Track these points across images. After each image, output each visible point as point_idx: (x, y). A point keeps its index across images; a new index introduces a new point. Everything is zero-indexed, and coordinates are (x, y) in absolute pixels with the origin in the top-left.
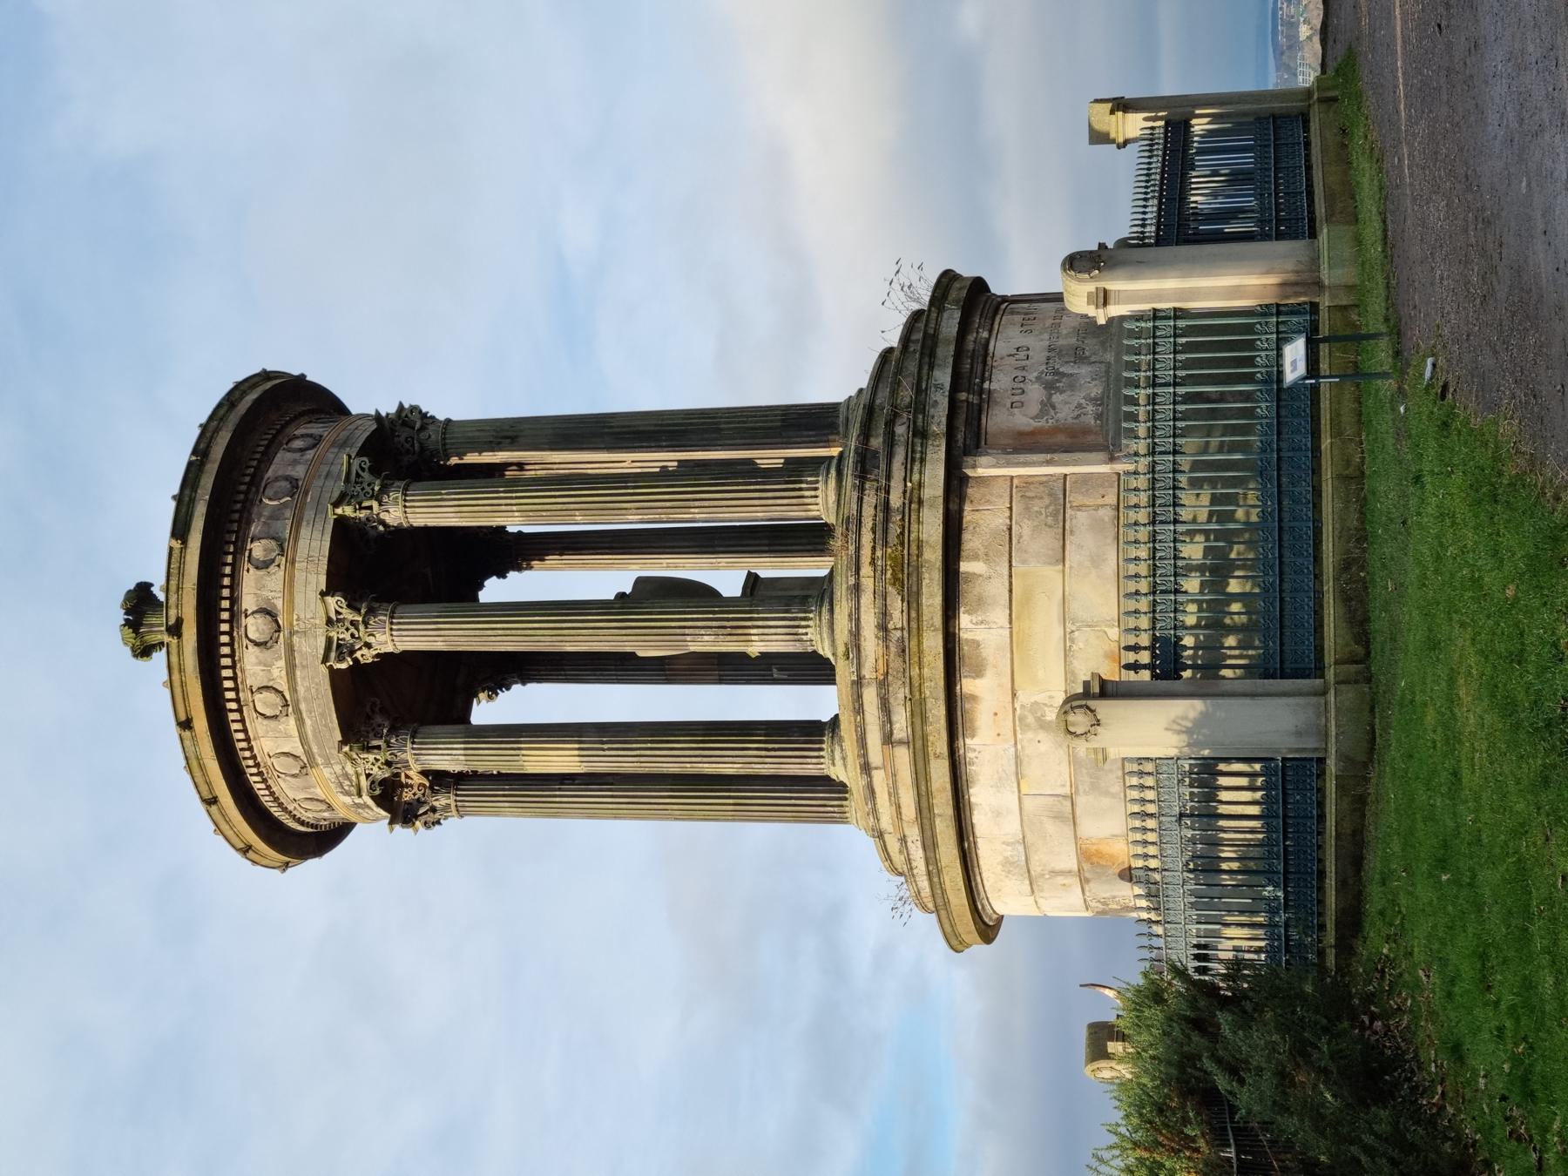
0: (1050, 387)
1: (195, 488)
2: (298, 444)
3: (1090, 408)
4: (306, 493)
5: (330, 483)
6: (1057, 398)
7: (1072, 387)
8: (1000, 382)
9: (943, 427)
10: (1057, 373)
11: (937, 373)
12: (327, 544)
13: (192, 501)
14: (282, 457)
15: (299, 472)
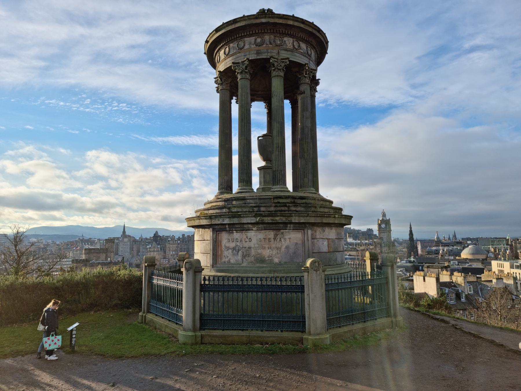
0: (234, 249)
1: (227, 26)
2: (259, 40)
3: (227, 260)
4: (239, 53)
5: (243, 57)
6: (230, 251)
7: (234, 255)
8: (236, 235)
9: (213, 223)
10: (239, 250)
11: (228, 219)
13: (224, 28)
14: (252, 39)
15: (247, 47)
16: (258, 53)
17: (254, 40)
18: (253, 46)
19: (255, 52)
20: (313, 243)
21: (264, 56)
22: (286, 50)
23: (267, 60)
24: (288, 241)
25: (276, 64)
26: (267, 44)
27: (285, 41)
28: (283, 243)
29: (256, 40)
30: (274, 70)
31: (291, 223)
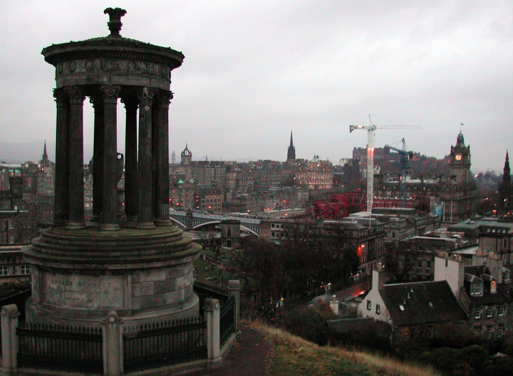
2: (89, 64)
8: (59, 277)
12: (61, 86)
14: (83, 63)
15: (78, 70)
16: (88, 79)
17: (84, 64)
18: (84, 70)
19: (86, 78)
20: (133, 287)
21: (93, 83)
22: (118, 75)
23: (98, 86)
24: (107, 286)
25: (107, 91)
26: (98, 69)
27: (118, 65)
28: (102, 287)
29: (86, 63)
30: (105, 97)
31: (108, 270)
